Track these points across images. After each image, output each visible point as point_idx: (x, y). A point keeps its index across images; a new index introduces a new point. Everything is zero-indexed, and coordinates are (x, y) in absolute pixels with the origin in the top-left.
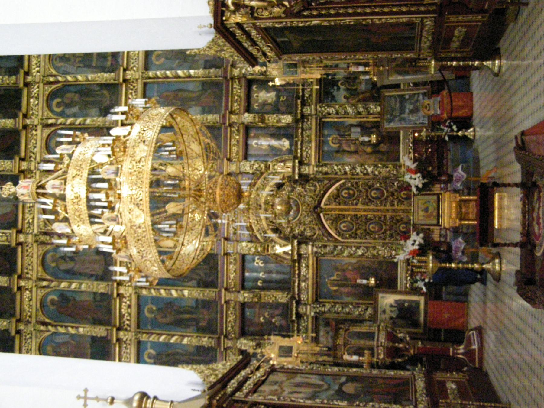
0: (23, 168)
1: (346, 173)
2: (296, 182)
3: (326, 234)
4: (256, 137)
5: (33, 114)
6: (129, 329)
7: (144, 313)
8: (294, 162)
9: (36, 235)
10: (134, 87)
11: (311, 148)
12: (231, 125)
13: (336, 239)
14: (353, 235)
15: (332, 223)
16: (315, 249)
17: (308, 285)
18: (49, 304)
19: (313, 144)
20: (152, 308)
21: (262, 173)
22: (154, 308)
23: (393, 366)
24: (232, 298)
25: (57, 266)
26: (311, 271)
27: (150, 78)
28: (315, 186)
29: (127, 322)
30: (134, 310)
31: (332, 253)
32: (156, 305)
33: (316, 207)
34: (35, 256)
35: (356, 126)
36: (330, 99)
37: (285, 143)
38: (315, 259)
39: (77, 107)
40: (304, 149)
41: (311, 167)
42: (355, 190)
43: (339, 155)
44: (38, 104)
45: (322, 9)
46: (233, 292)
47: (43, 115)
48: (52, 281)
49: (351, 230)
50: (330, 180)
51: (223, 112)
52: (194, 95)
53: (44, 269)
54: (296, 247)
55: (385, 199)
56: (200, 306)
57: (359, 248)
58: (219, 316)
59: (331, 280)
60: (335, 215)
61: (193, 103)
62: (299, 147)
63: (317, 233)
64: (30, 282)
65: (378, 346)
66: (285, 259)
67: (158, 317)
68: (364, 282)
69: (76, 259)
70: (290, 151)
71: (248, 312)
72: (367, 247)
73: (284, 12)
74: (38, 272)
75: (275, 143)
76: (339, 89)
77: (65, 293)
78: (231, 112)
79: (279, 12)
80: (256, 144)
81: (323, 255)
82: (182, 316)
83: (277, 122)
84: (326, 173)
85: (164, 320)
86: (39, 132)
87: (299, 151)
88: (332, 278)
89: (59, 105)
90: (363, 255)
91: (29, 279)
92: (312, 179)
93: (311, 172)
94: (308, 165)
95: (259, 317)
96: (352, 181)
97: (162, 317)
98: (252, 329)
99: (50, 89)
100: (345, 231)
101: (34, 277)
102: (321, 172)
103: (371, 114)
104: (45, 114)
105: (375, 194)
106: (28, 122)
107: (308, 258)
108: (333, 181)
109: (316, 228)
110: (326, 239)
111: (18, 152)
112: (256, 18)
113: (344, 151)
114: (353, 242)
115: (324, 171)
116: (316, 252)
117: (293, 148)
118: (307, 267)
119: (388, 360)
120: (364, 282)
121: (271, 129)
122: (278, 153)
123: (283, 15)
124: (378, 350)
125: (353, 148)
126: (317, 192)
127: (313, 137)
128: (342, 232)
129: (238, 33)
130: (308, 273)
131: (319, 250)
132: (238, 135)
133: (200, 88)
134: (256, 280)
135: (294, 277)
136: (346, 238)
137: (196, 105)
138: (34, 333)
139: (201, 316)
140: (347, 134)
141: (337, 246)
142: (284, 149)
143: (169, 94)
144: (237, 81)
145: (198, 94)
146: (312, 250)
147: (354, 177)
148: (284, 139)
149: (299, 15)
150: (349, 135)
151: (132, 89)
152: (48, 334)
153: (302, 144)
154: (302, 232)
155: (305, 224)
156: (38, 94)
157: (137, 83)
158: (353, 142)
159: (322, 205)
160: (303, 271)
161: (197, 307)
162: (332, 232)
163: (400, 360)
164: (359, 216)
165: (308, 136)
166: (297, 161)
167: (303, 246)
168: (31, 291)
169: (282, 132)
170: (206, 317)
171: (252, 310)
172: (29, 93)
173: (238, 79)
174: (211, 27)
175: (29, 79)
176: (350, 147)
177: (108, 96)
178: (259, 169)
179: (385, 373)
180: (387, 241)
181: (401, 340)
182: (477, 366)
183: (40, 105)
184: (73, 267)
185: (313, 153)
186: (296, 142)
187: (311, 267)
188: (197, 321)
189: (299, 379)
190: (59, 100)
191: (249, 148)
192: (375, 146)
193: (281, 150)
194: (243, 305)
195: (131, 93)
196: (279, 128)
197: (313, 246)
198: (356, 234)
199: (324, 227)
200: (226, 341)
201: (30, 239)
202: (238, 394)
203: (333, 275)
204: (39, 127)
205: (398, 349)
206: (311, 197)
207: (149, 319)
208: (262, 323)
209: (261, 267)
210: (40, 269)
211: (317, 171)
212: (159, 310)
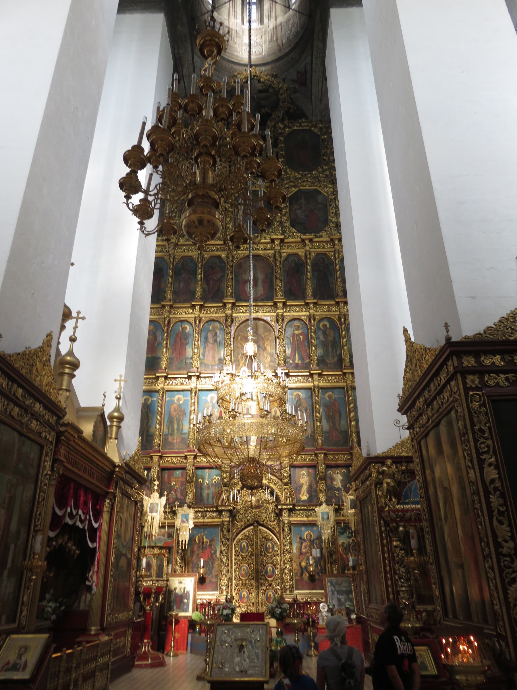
0: (278, 304)
1: (285, 546)
2: (276, 506)
3: (238, 531)
4: (309, 474)
5: (316, 308)
6: (166, 384)
7: (178, 394)
8: (290, 505)
9: (231, 315)
10: (341, 380)
11: (302, 517)
12: (316, 455)
13: (234, 539)
14: (238, 553)
15: (246, 536)
16: (226, 523)
17: (199, 519)
18: (183, 326)
19: (305, 519)
21: (281, 480)
22: (181, 402)
23: (137, 593)
24: (189, 461)
25: (210, 330)
26: (210, 520)
27: (348, 392)
28: (274, 521)
29: (171, 382)
30: (180, 387)
31: (224, 537)
32: (184, 402)
33: (257, 522)
34: (217, 315)
35: (321, 552)
36: (341, 531)
37: (304, 497)
38: (220, 523)
39: (323, 339)
40: (301, 512)
41: (287, 518)
42: (272, 554)
43: (298, 540)
44: (324, 311)
45: (386, 535)
46: (194, 461)
47: (317, 315)
48: (199, 327)
49: (242, 552)
50: (279, 533)
51: (326, 447)
52: (337, 425)
53: (207, 322)
54: (227, 508)
55: (266, 579)
57: (228, 559)
58: (176, 450)
60: (253, 538)
61: (331, 425)
62: (302, 508)
63: (239, 524)
64: (198, 313)
65: (152, 580)
66: (219, 500)
67: (175, 405)
68: (202, 564)
69: (216, 344)
70: (299, 500)
71: (178, 473)
72: (228, 565)
73: (382, 506)
74: (205, 317)
75: (305, 489)
76: (349, 538)
77: (192, 337)
78: (325, 455)
79: (382, 503)
80: (304, 474)
81: (222, 531)
83: (321, 490)
84: (283, 530)
85: (172, 409)
86: (304, 313)
87: (299, 508)
88: (204, 538)
89: (324, 326)
90: (222, 562)
91: (200, 312)
92: (279, 519)
93: (283, 518)
94: (289, 515)
95: (175, 482)
96: (279, 551)
97: (174, 409)
98: (166, 476)
99: (336, 319)
100: (241, 546)
101: (201, 315)
102: (284, 526)
103: (331, 565)
104: (317, 317)
105: (270, 570)
106: (312, 305)
107: (220, 518)
108: (278, 536)
109: (243, 523)
110: (234, 531)
111: (289, 299)
112: (376, 487)
113: (302, 544)
114: (232, 553)
115: (285, 528)
116: (223, 524)
117: (301, 503)
118: (213, 518)
119: (142, 590)
120: (202, 564)
121: (315, 485)
122: (298, 491)
123: (379, 505)
124: (149, 581)
125: (304, 550)
126: (269, 522)
127: (311, 519)
128: (239, 544)
129: (368, 472)
130: (208, 518)
131: (226, 527)
132: (309, 460)
133: (343, 429)
134: (203, 479)
135: (205, 507)
136: (235, 548)
137: (330, 426)
138: (163, 316)
139: (176, 438)
140: (315, 545)
141: (228, 540)
142: (301, 496)
143: (337, 406)
144: (349, 457)
145: (338, 428)
146: (226, 521)
147: (282, 552)
148: (308, 495)
149: (380, 517)
150: (314, 548)
151: (339, 379)
152: (163, 326)
153: (304, 510)
154: (239, 512)
155: (245, 514)
156: (331, 311)
157: (343, 382)
158: (309, 551)
159: (260, 527)
160: (211, 514)
161: (182, 434)
162: (240, 536)
163: (142, 599)
164: (253, 557)
165: (311, 515)
166: (291, 507)
167: (228, 514)
168: (192, 313)
169: (313, 493)
170: (175, 441)
171: (180, 475)
172: (332, 305)
173: (351, 458)
174: (368, 455)
175: (342, 305)
176: (305, 548)
177: (333, 361)
178: (284, 478)
179: (133, 588)
180: (234, 581)
181: (157, 599)
182: (136, 663)
183: (323, 313)
184: (208, 342)
185: (298, 519)
186: (306, 506)
187: (212, 520)
188: (172, 434)
189: (131, 523)
190: (328, 325)
191: (300, 469)
192: (306, 568)
193: (300, 493)
194: (184, 468)
195: (336, 378)
196: (316, 491)
197: (229, 521)
198: (238, 556)
199: (243, 529)
200: (158, 457)
201: (229, 312)
202: (122, 482)
204: (307, 313)
205: (149, 597)
206: (266, 518)
207: (172, 399)
208: (170, 483)
209: (212, 480)
210: (208, 319)
211: (284, 523)
212: (180, 406)
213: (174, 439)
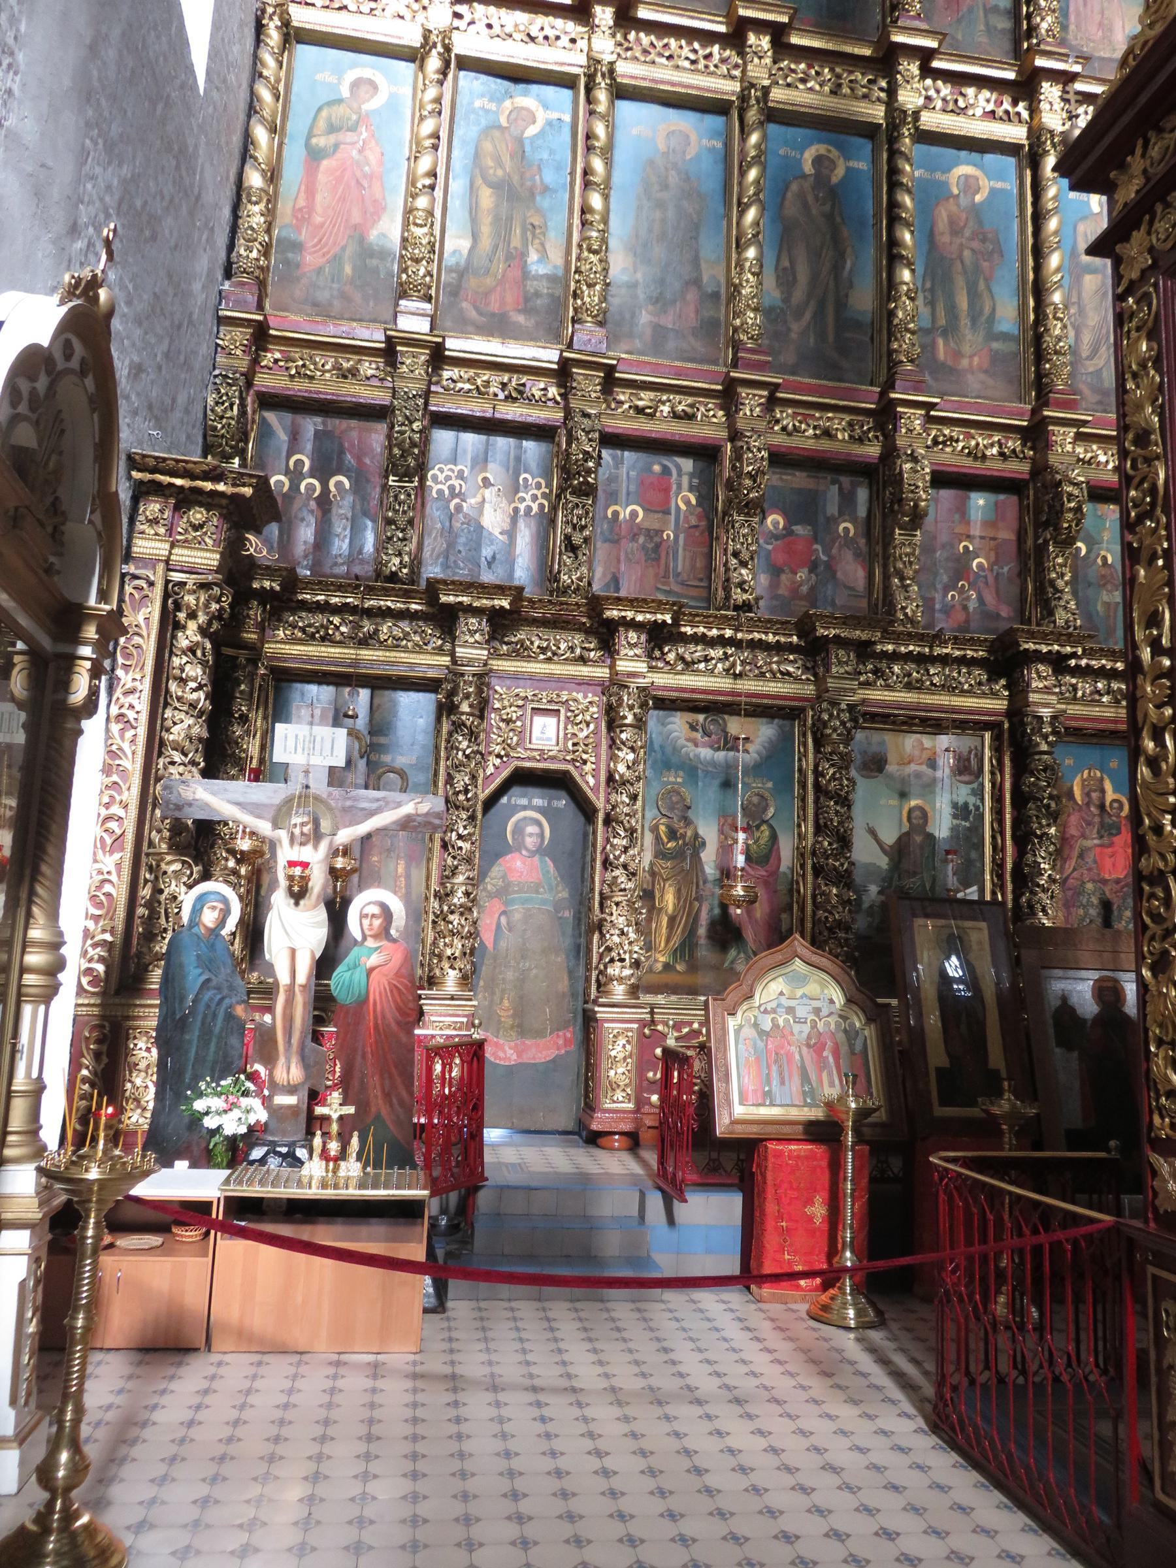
20: (977, 191)
22: (978, 198)
56: (996, 345)
59: (1102, 779)
82: (960, 282)
85: (942, 224)
88: (1108, 786)
97: (952, 222)
139: (967, 349)
170: (965, 363)
188: (951, 330)
203: (1115, 790)
213: (958, 355)
